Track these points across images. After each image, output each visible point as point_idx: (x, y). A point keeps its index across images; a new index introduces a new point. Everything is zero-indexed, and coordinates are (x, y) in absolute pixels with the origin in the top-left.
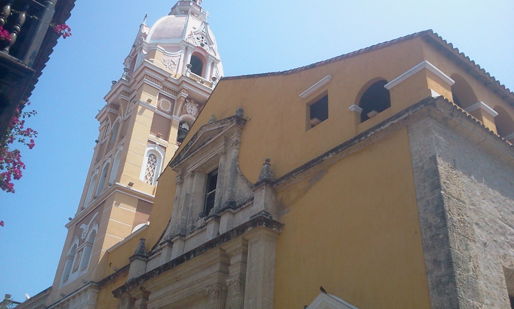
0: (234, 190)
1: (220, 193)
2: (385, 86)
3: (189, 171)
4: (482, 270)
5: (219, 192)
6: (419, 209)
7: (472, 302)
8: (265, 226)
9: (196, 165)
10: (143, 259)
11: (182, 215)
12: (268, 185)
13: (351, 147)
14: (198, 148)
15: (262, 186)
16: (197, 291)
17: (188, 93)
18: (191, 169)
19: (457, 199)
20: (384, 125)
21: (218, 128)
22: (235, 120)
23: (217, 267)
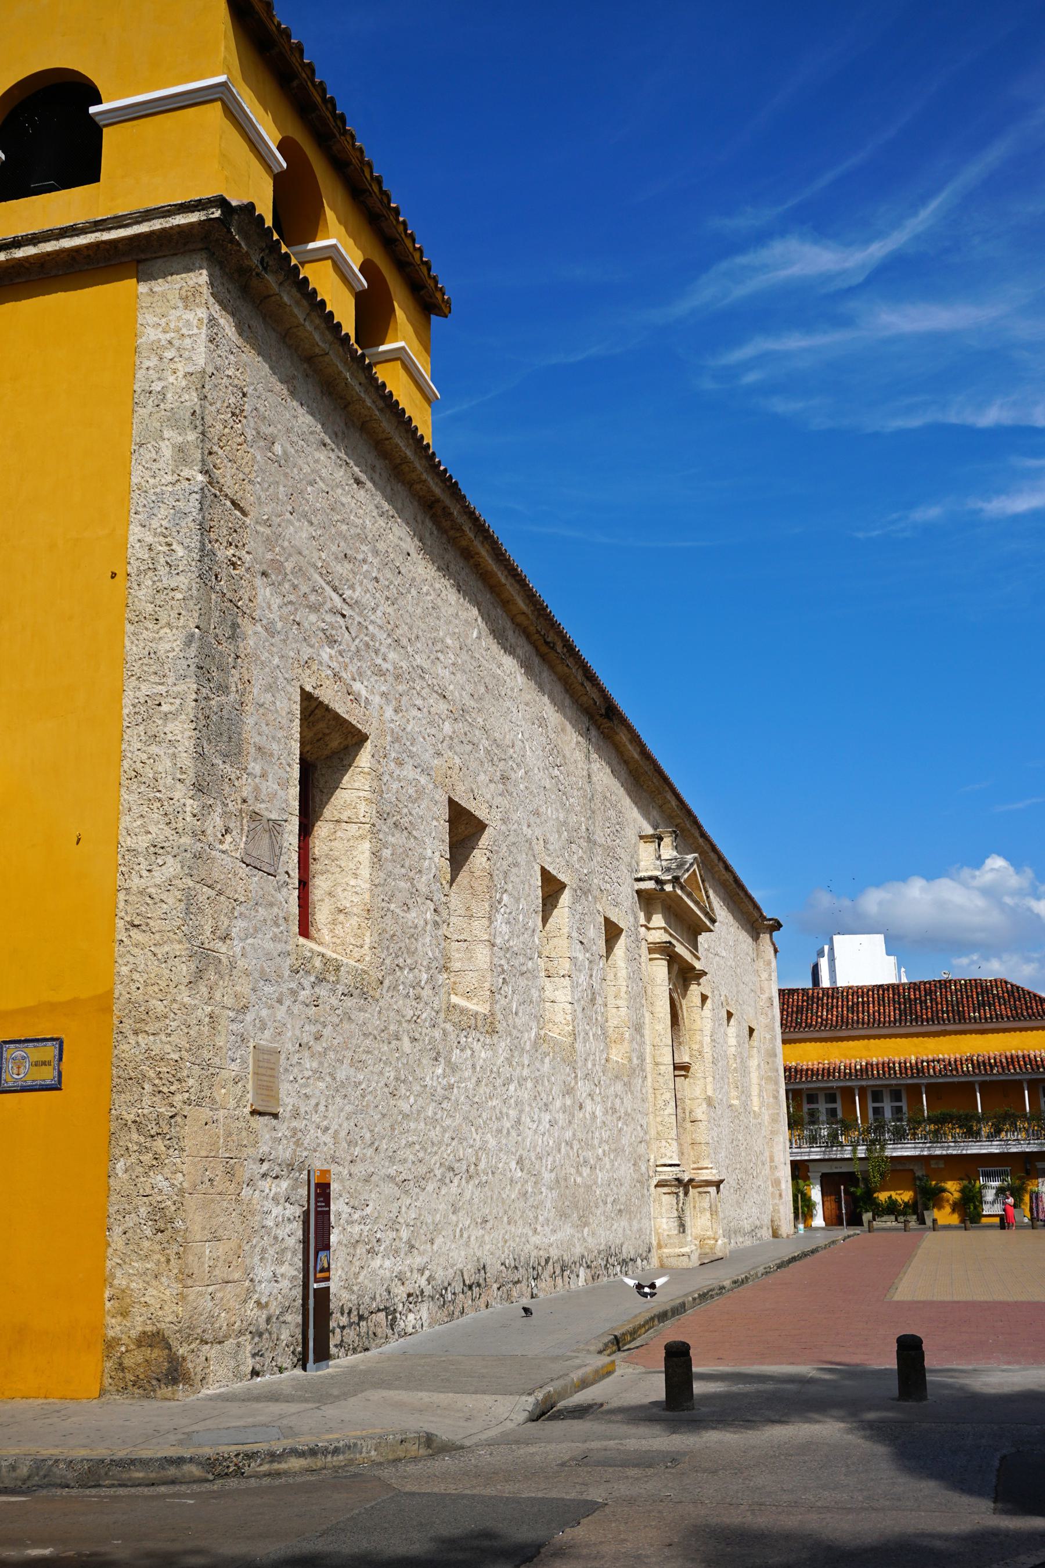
4: (255, 691)
6: (133, 511)
7: (222, 767)
19: (233, 503)
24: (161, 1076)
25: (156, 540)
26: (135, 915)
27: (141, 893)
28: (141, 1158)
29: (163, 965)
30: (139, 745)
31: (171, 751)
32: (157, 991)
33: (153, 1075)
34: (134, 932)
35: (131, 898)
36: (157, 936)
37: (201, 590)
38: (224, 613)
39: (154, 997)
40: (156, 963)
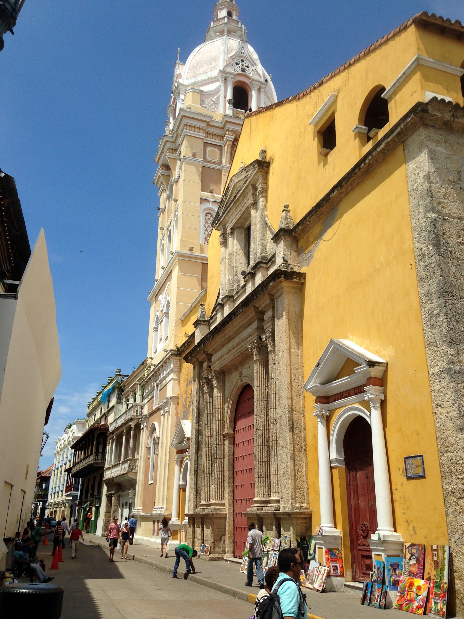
0: (265, 243)
1: (254, 248)
2: (382, 96)
3: (229, 231)
5: (253, 247)
8: (283, 279)
9: (233, 221)
10: (204, 323)
11: (229, 276)
12: (286, 234)
13: (353, 178)
14: (231, 203)
15: (281, 237)
16: (244, 350)
17: (234, 135)
18: (230, 226)
20: (379, 146)
21: (245, 177)
22: (256, 165)
23: (255, 325)
24: (457, 471)
25: (423, 246)
26: (438, 401)
27: (439, 391)
28: (456, 508)
29: (451, 422)
30: (429, 330)
31: (439, 330)
32: (450, 433)
33: (455, 471)
34: (439, 408)
35: (436, 394)
36: (447, 409)
37: (441, 261)
38: (460, 265)
39: (450, 436)
40: (448, 421)
